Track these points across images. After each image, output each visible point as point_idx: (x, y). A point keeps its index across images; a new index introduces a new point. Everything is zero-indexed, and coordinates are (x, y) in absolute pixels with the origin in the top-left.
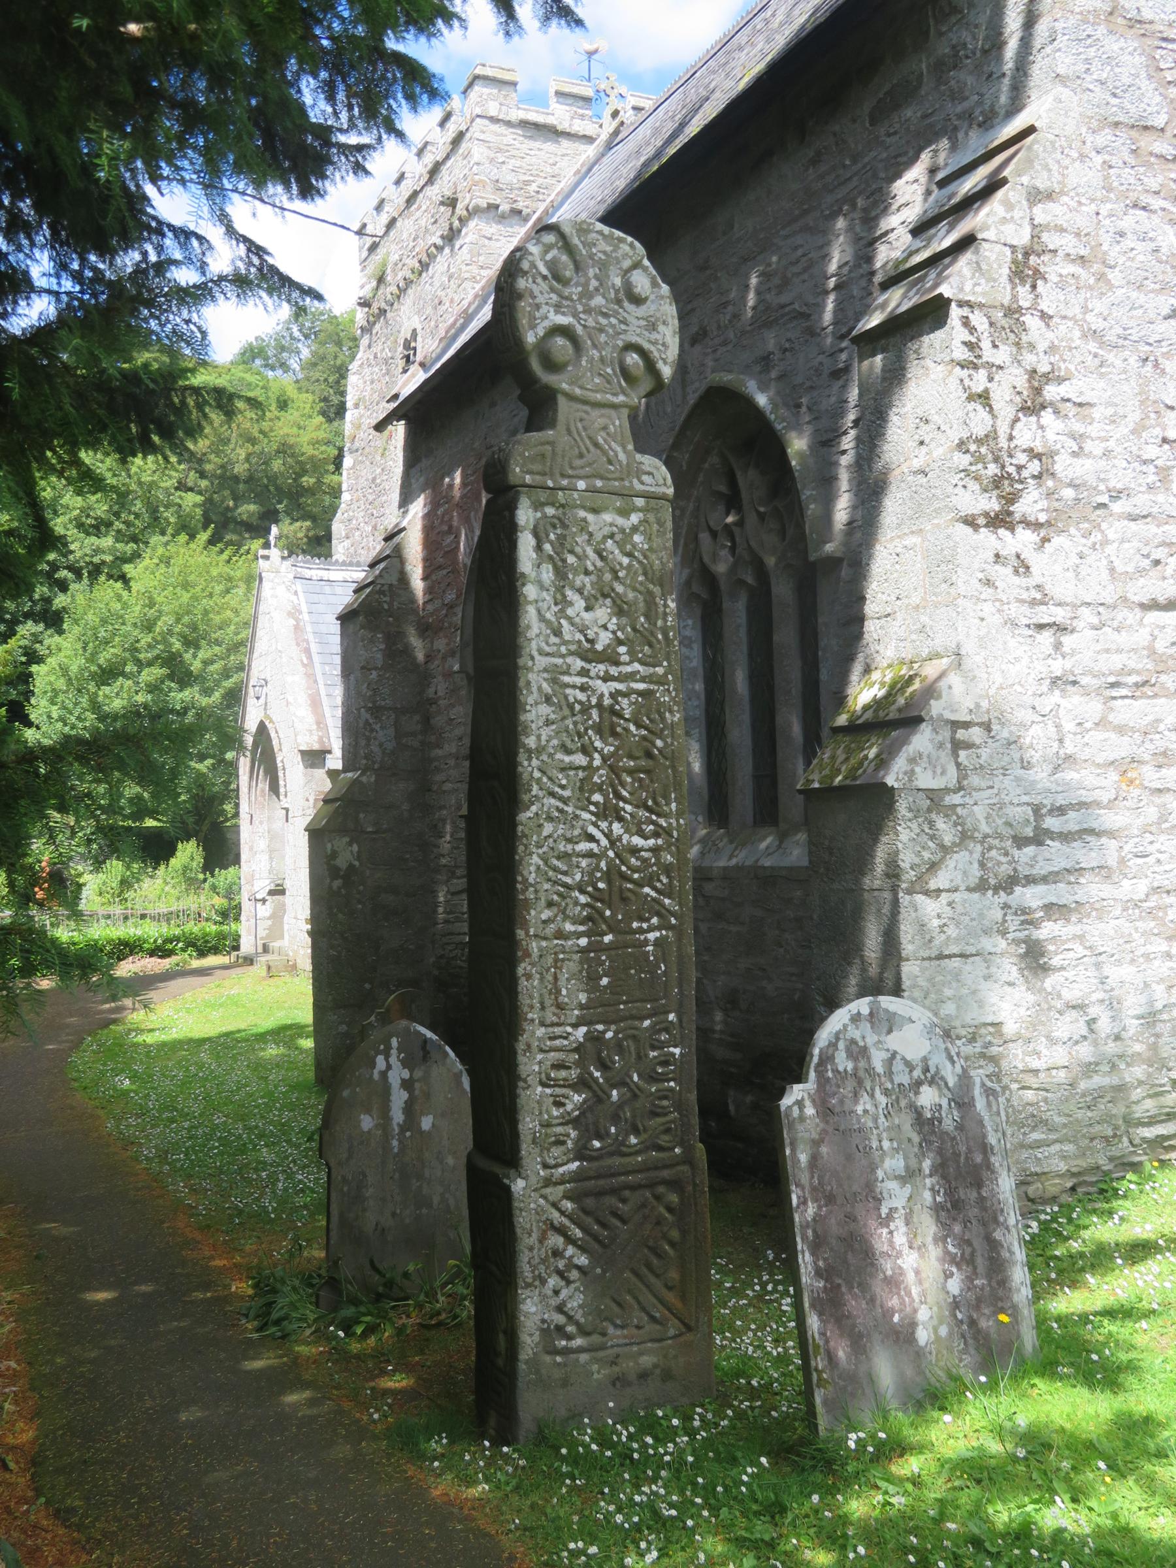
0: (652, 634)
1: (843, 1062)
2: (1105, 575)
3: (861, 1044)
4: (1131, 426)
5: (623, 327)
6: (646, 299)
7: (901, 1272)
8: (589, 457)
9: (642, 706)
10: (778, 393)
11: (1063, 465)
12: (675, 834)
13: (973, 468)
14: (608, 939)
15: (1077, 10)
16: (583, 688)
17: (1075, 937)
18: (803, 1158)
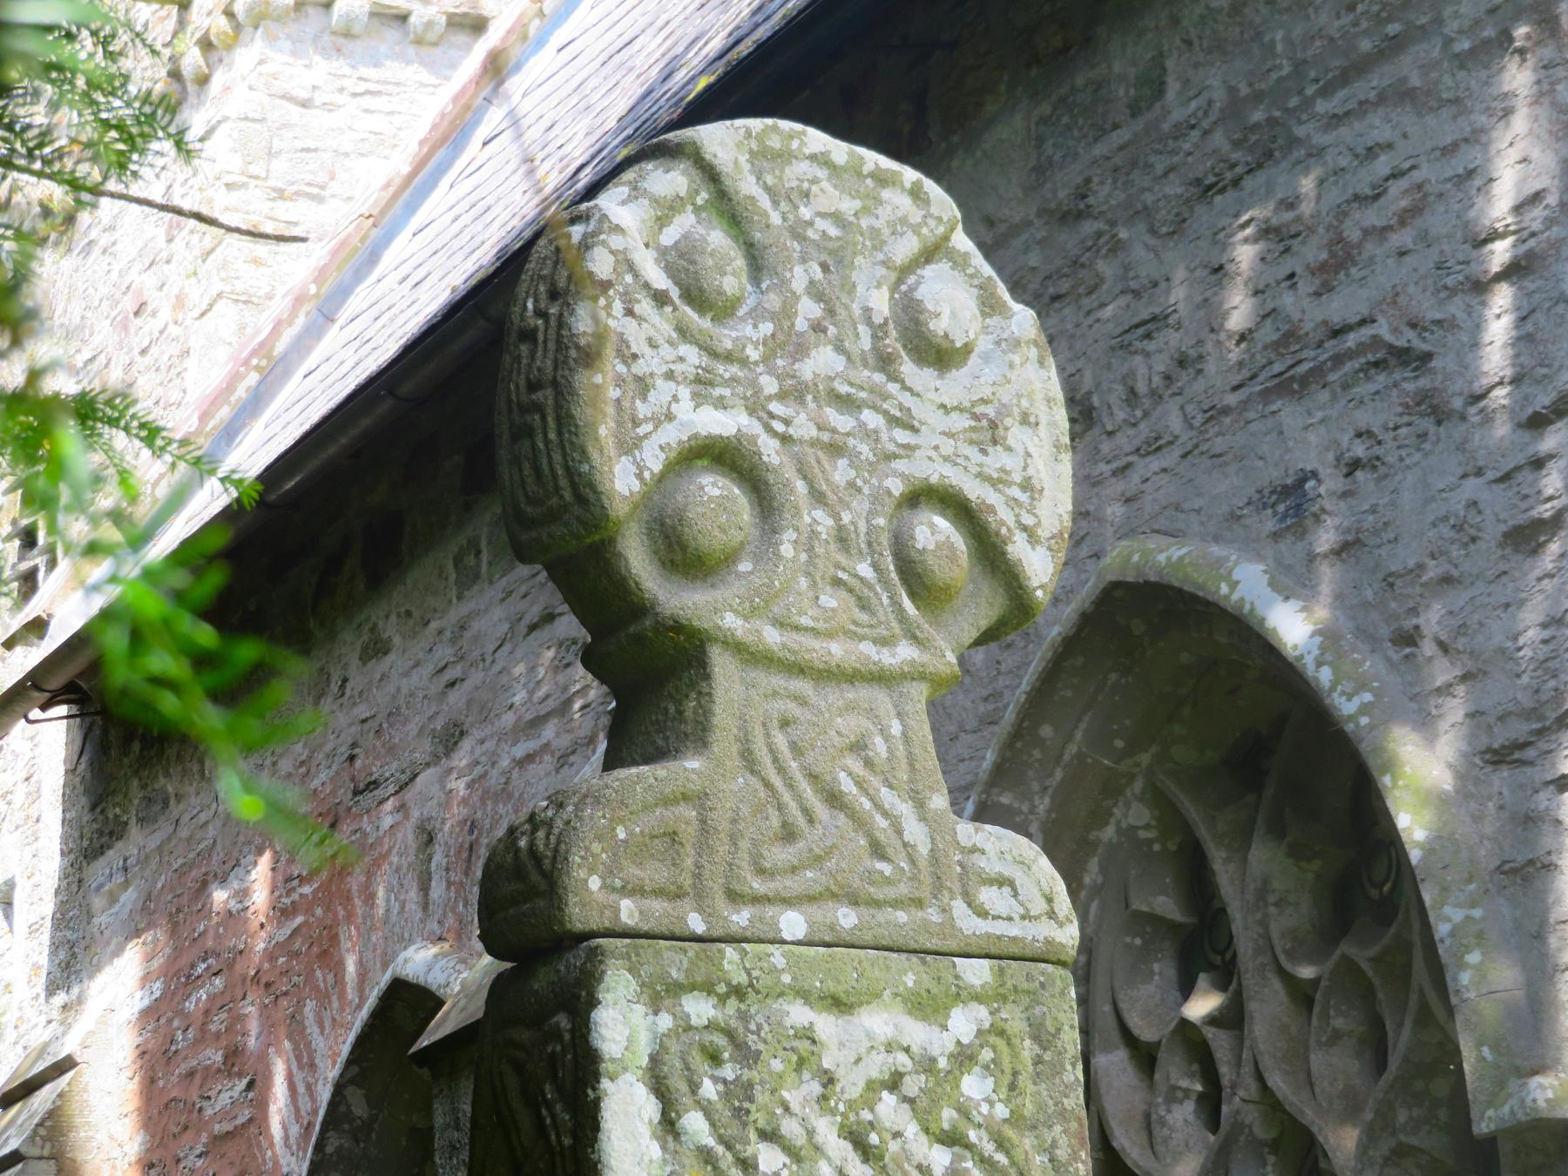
5: (902, 436)
6: (967, 349)
8: (812, 838)
10: (1339, 598)
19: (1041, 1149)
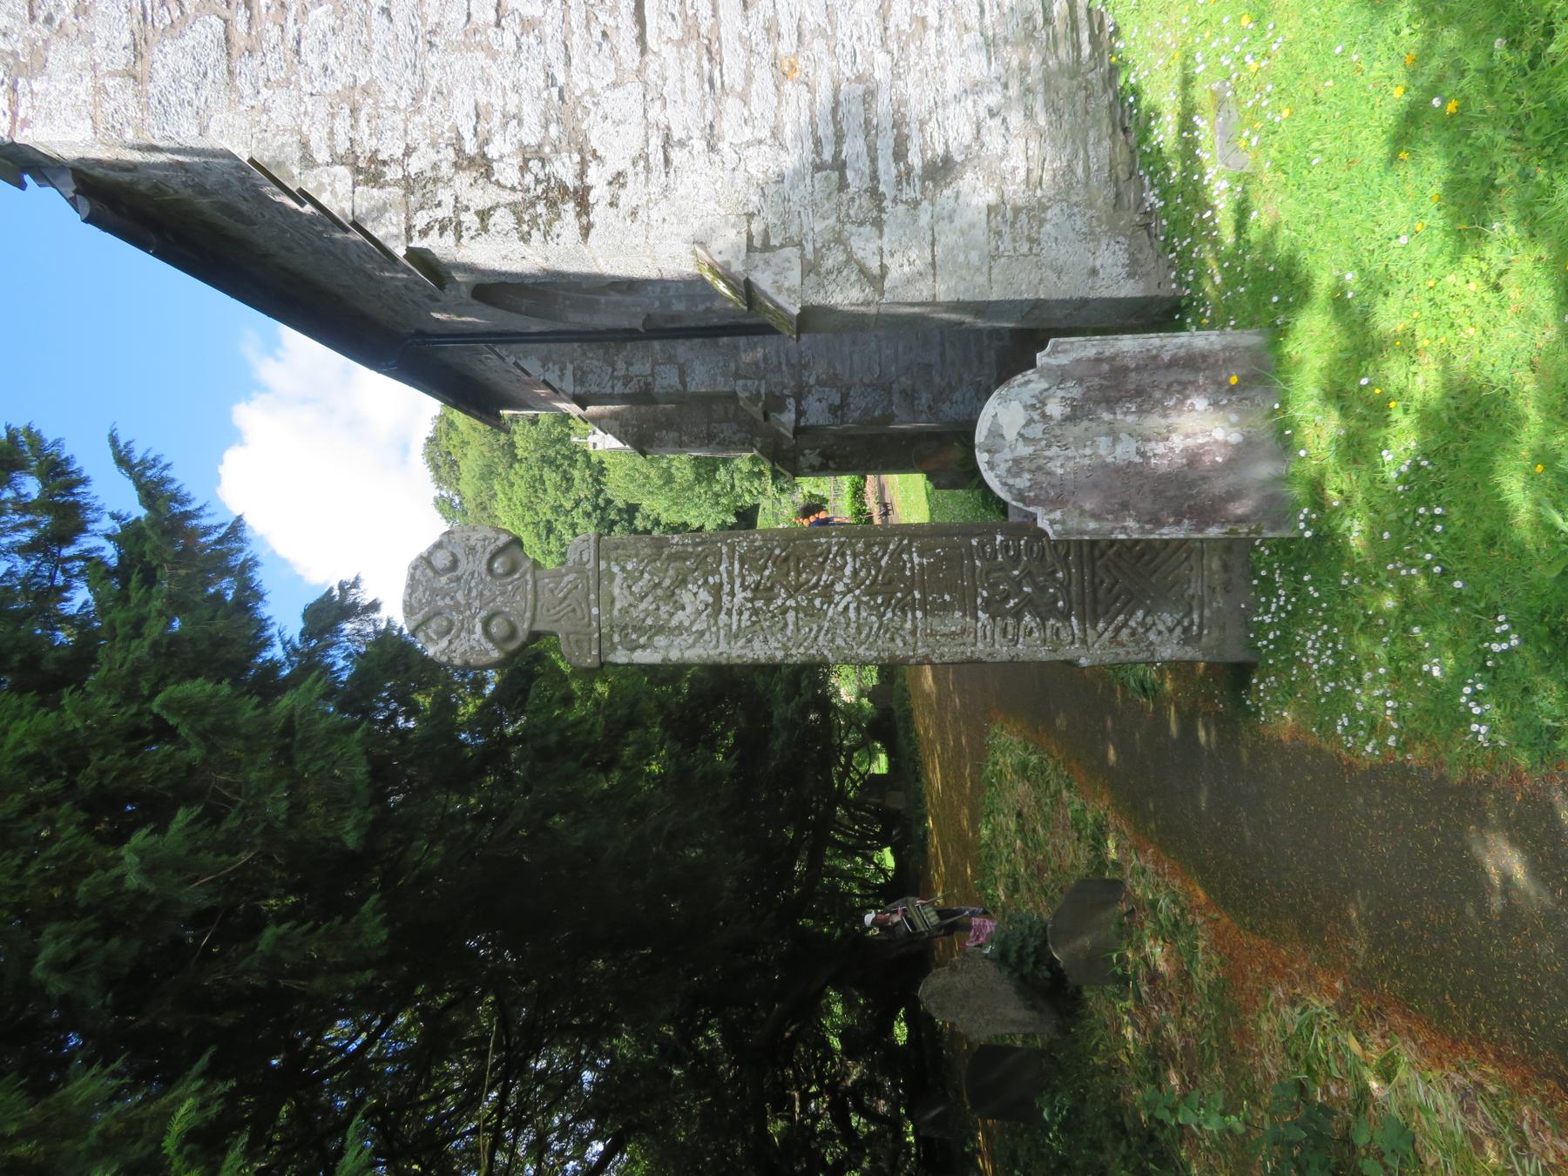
0: (698, 556)
1: (1023, 482)
2: (619, 93)
4: (490, 61)
6: (453, 555)
7: (1185, 450)
8: (575, 604)
9: (751, 566)
11: (531, 137)
12: (843, 539)
13: (542, 227)
14: (917, 595)
15: (139, 115)
16: (740, 613)
17: (921, 130)
18: (1092, 525)
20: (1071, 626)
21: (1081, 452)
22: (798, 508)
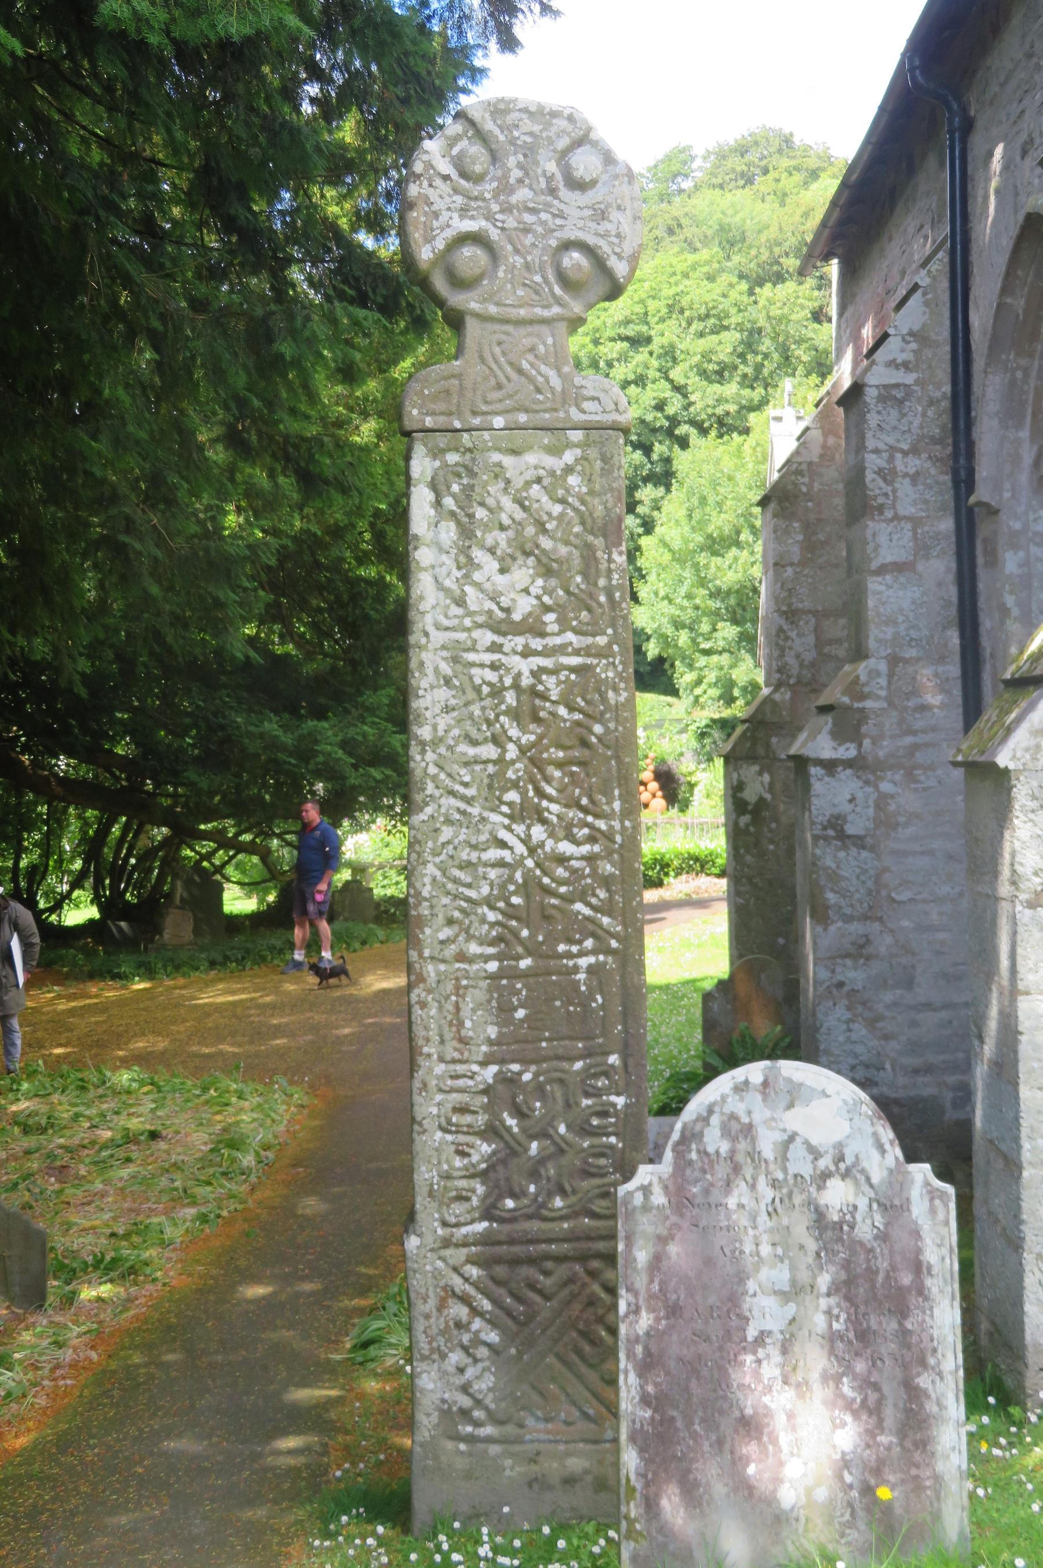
0: (591, 596)
1: (714, 1140)
3: (745, 1120)
5: (559, 221)
6: (594, 183)
7: (768, 1413)
8: (509, 388)
9: (574, 684)
12: (618, 838)
14: (525, 963)
16: (494, 667)
18: (642, 1256)
19: (601, 503)
20: (472, 1222)
21: (765, 1238)
22: (670, 760)
